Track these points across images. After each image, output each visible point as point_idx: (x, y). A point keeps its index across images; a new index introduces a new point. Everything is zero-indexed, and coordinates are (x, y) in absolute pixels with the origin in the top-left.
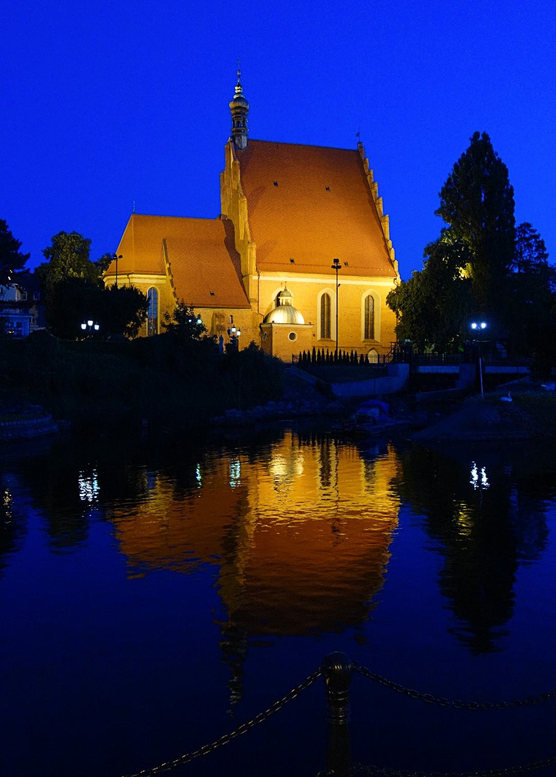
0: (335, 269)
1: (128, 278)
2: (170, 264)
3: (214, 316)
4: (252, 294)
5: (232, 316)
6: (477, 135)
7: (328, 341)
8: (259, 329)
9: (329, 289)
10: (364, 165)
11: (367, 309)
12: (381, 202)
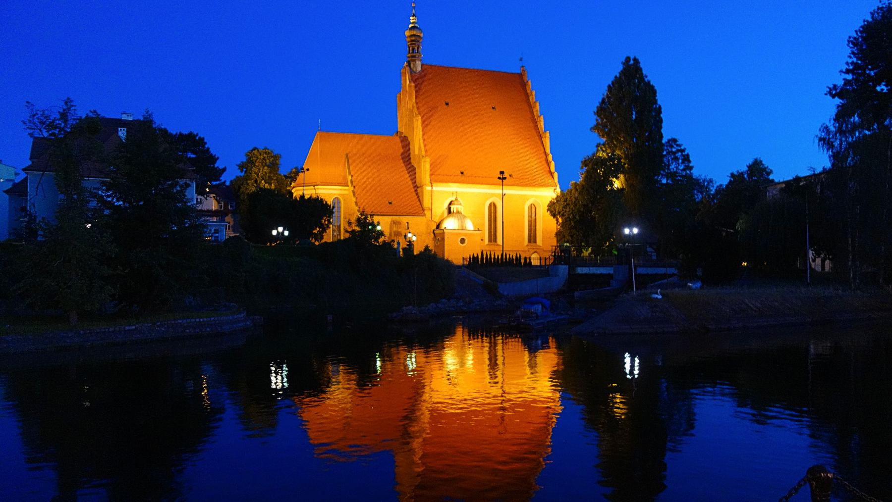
0: (501, 180)
1: (314, 189)
2: (352, 176)
3: (392, 223)
4: (426, 203)
5: (408, 223)
6: (628, 59)
7: (494, 245)
8: (433, 235)
9: (496, 198)
10: (527, 87)
11: (530, 216)
12: (542, 120)
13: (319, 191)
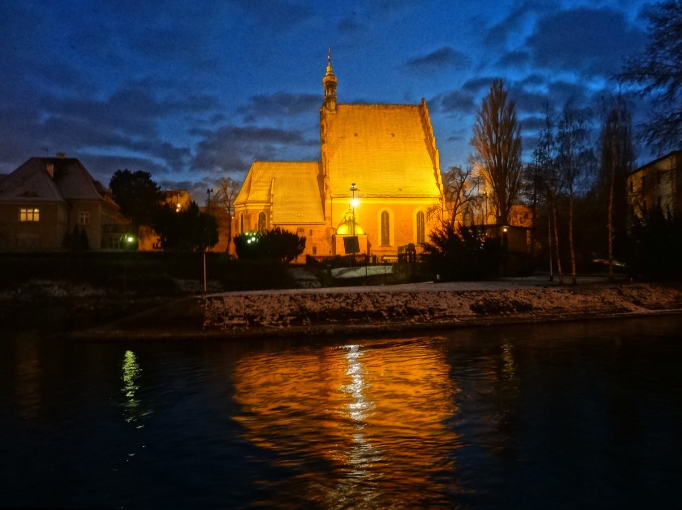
0: (352, 192)
8: (331, 239)
13: (248, 208)
